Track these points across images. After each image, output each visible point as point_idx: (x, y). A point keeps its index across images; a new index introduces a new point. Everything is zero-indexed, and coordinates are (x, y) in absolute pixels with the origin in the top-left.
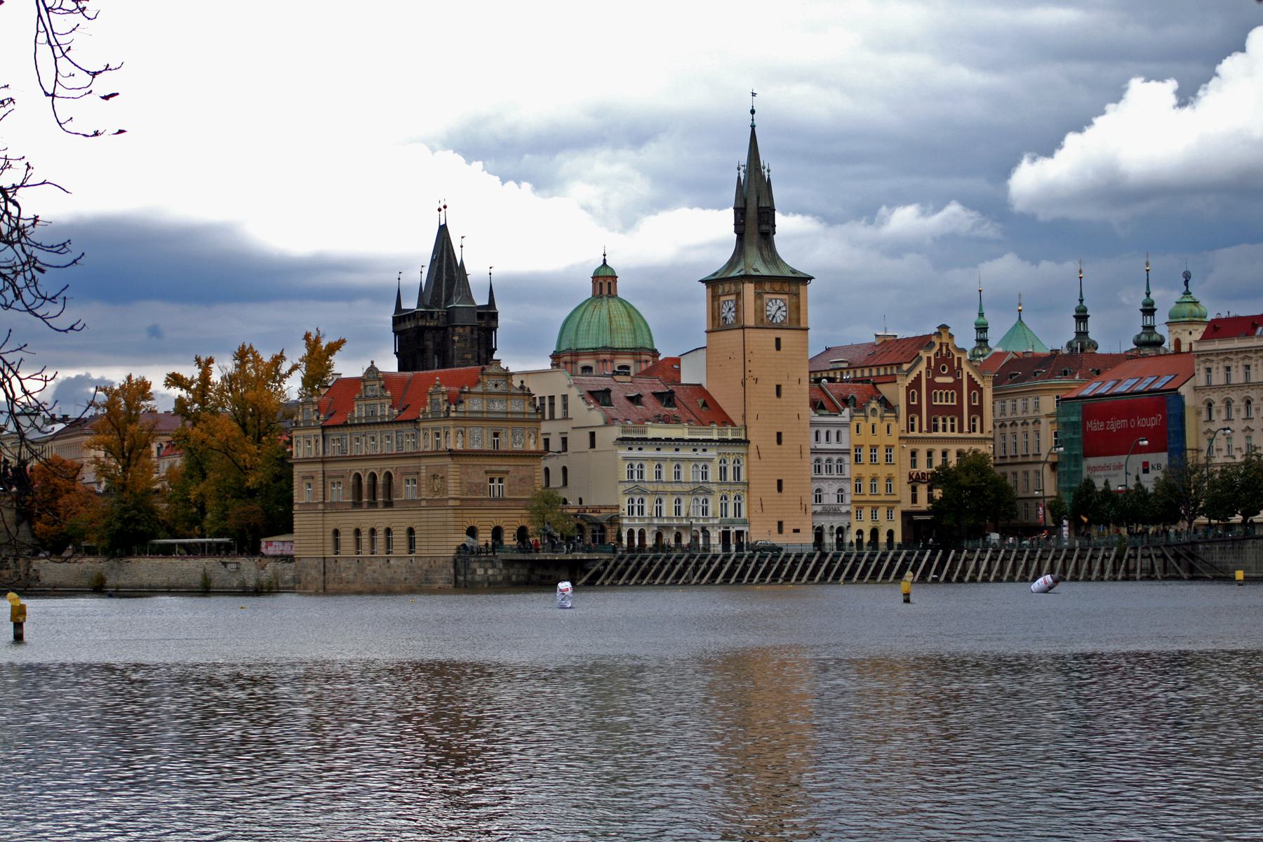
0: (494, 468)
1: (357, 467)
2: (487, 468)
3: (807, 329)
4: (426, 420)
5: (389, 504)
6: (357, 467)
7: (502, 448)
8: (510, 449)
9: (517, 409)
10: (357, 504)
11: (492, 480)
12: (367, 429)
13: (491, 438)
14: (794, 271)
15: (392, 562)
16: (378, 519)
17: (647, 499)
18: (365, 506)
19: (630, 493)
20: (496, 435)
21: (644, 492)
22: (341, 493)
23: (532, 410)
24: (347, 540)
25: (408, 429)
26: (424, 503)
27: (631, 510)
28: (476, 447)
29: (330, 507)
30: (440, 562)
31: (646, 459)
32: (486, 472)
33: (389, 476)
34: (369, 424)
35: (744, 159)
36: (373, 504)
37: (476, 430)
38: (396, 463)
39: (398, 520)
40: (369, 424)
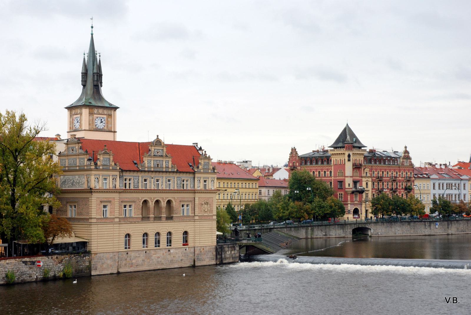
1: (146, 196)
3: (115, 132)
4: (200, 173)
5: (170, 218)
6: (146, 196)
10: (145, 218)
12: (153, 175)
14: (111, 105)
15: (172, 251)
16: (164, 227)
18: (152, 219)
22: (135, 212)
24: (136, 242)
25: (189, 177)
26: (196, 218)
29: (125, 220)
30: (207, 249)
33: (169, 202)
34: (156, 172)
35: (87, 49)
36: (158, 218)
38: (176, 195)
39: (177, 228)
40: (156, 172)
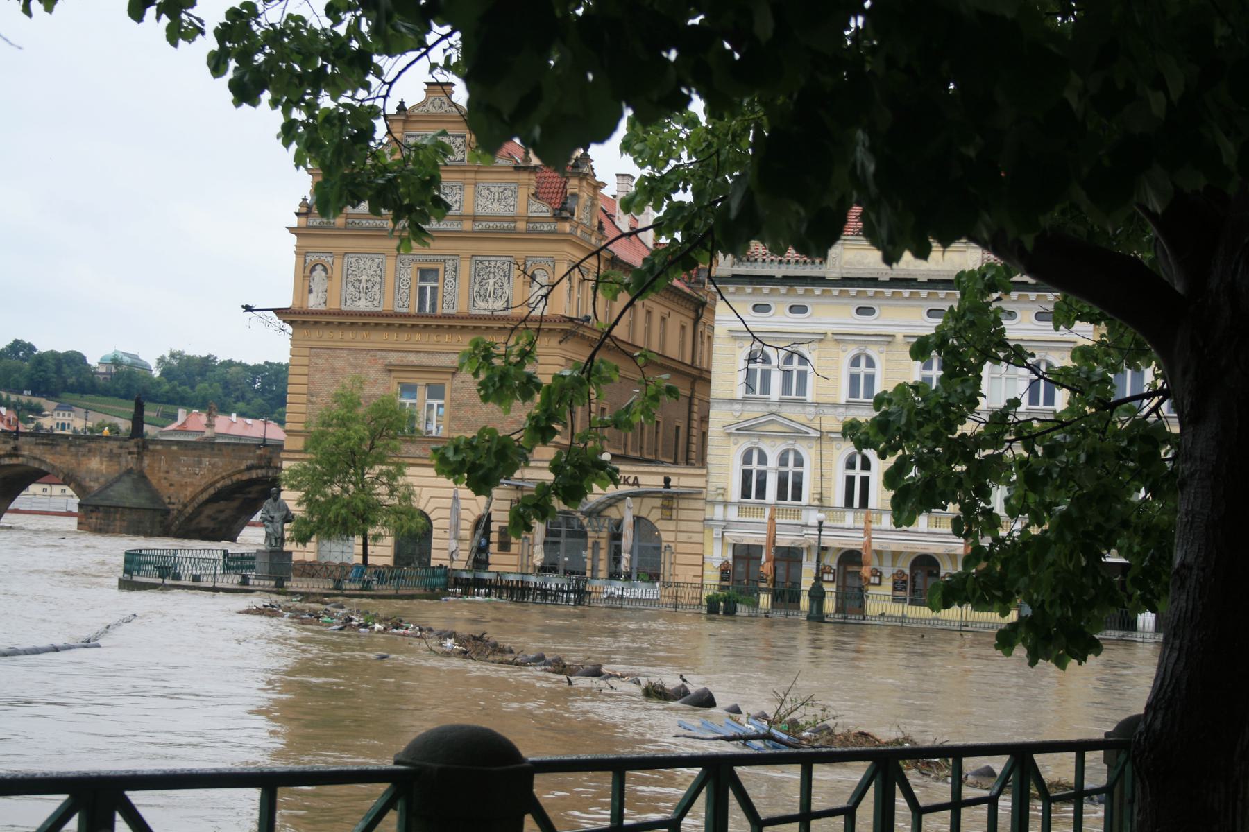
0: (413, 359)
2: (393, 358)
7: (439, 311)
8: (461, 307)
9: (496, 208)
11: (409, 389)
13: (410, 275)
17: (809, 453)
19: (744, 430)
20: (425, 274)
21: (799, 434)
23: (543, 209)
27: (752, 486)
28: (363, 305)
31: (821, 338)
32: (390, 369)
37: (365, 263)
